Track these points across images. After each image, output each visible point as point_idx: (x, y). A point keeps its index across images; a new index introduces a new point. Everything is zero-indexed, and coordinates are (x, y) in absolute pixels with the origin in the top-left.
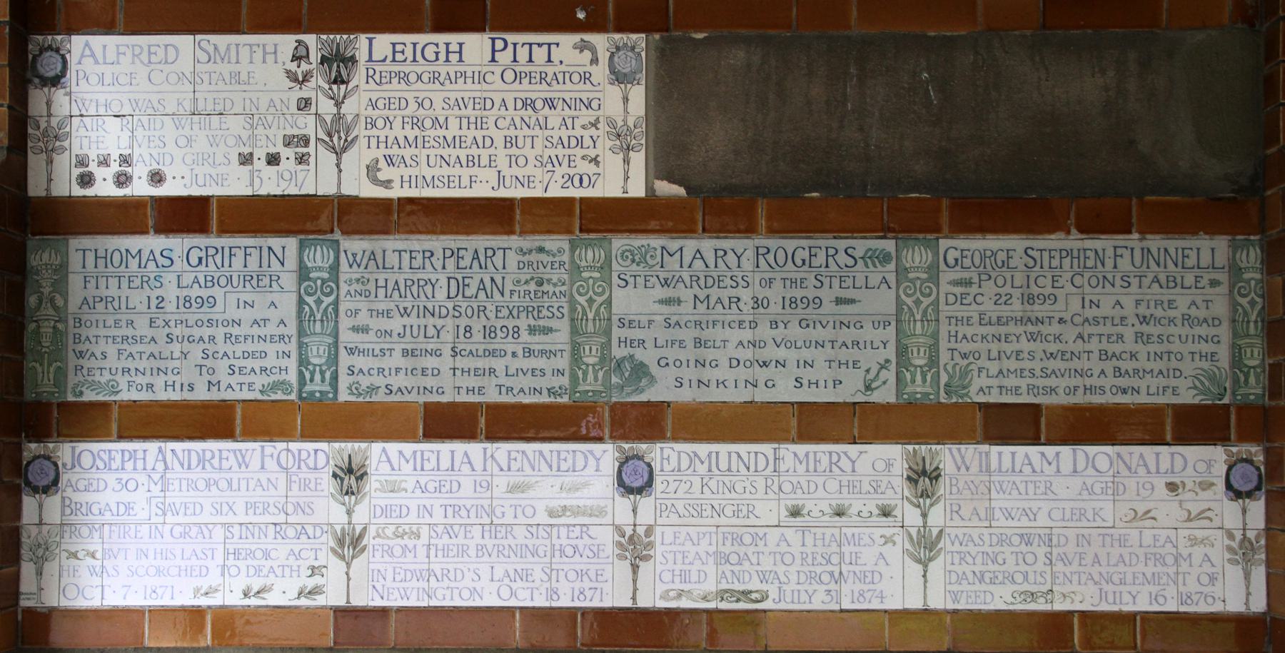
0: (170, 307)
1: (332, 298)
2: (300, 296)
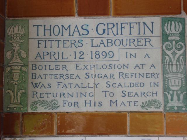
0: (87, 57)
1: (182, 51)
2: (163, 51)
